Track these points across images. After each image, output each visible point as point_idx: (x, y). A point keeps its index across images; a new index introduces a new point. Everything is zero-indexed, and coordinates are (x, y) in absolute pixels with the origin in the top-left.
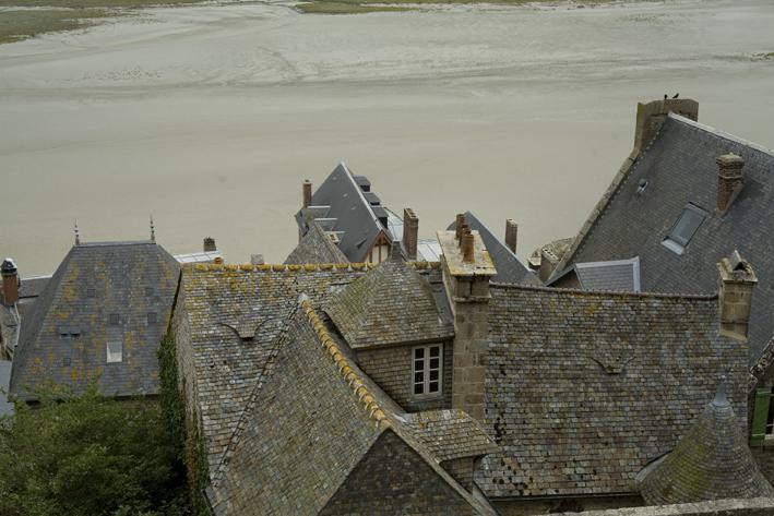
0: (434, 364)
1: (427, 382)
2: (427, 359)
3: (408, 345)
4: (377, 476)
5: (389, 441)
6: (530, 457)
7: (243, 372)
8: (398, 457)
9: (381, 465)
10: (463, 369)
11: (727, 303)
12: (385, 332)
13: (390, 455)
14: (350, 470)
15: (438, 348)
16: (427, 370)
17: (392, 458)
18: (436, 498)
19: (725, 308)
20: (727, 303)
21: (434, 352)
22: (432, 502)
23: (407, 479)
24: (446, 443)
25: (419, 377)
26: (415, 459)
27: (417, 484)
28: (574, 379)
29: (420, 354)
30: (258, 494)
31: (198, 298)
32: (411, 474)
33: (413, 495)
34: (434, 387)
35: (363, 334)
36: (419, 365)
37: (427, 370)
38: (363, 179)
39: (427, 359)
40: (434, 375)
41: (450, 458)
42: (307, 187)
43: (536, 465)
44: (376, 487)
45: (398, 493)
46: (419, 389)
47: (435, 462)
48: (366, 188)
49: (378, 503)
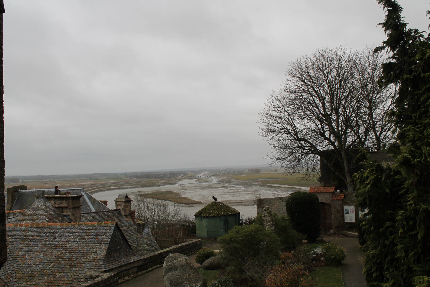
11: (126, 209)
19: (125, 211)
20: (126, 209)
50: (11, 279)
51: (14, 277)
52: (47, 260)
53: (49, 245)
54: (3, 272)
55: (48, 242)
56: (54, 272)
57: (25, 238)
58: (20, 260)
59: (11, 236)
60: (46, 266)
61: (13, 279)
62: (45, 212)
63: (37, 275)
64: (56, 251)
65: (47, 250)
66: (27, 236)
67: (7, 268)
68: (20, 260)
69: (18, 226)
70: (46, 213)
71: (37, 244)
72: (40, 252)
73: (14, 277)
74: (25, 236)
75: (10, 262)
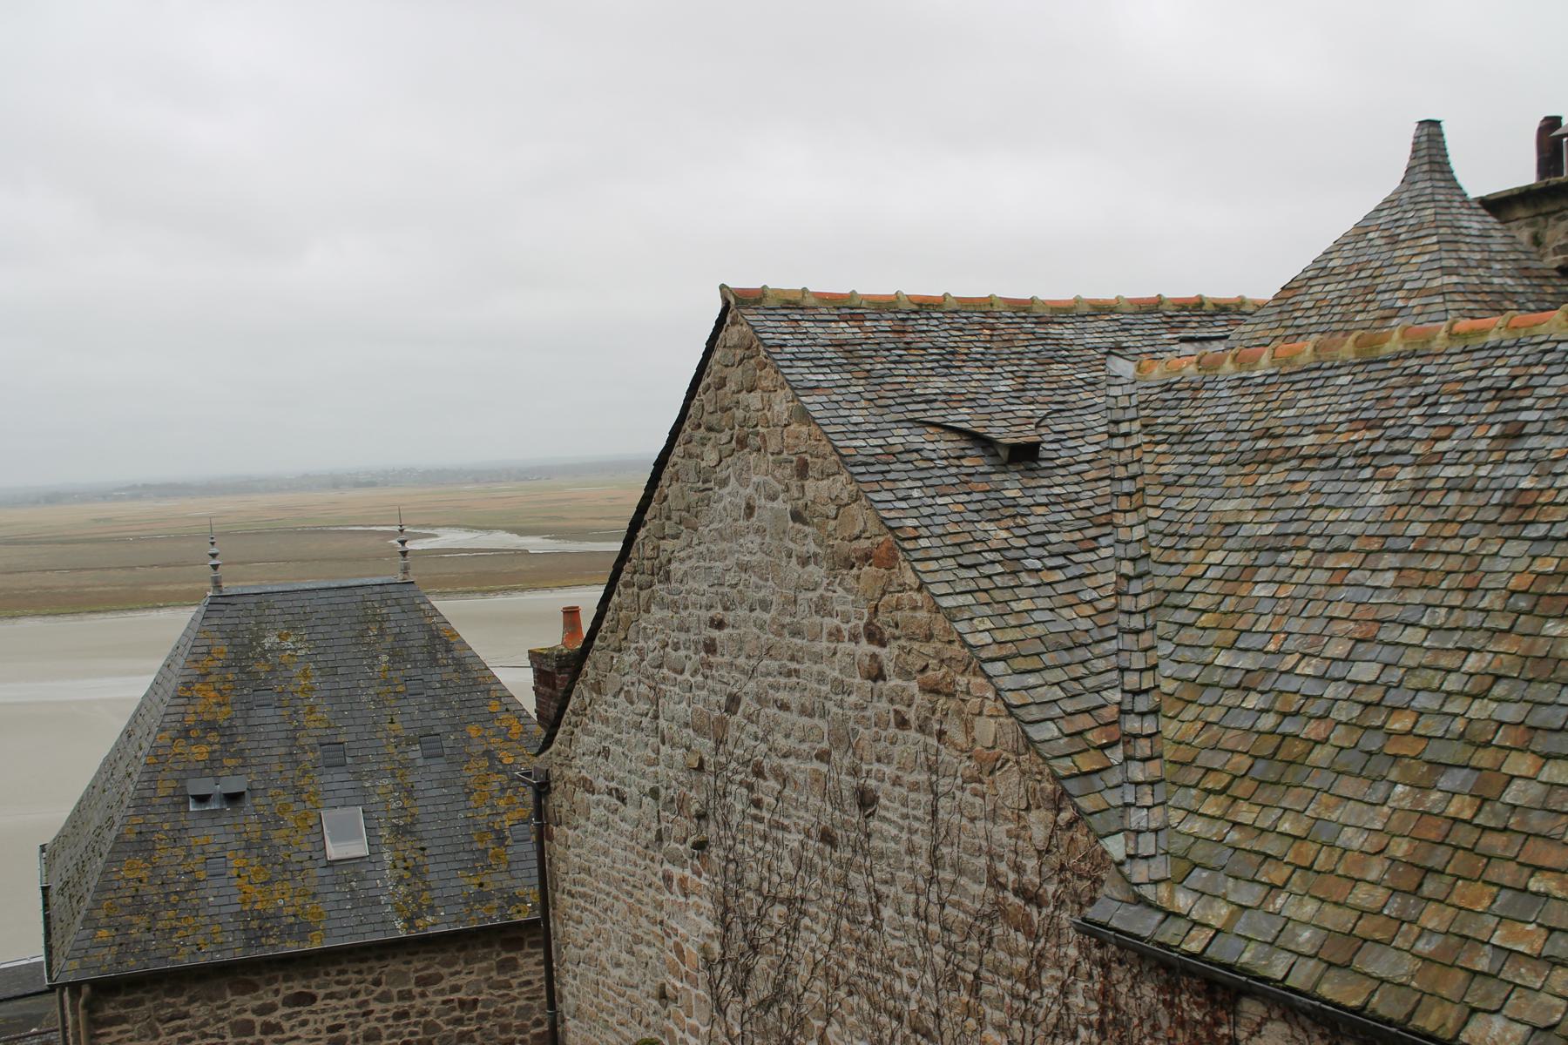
7: (1053, 538)
31: (817, 362)
50: (1116, 755)
51: (1143, 748)
52: (1430, 629)
53: (1453, 498)
54: (1062, 695)
55: (1450, 472)
56: (1488, 744)
57: (1262, 444)
58: (1204, 611)
59: (1174, 439)
60: (1414, 682)
61: (1128, 758)
62: (1447, 271)
63: (1320, 755)
64: (1512, 548)
65: (1428, 537)
66: (1278, 431)
67: (1101, 665)
68: (1204, 611)
69: (1228, 367)
70: (1455, 279)
71: (1348, 487)
72: (1368, 553)
73: (1143, 748)
74: (1268, 434)
75: (1137, 622)
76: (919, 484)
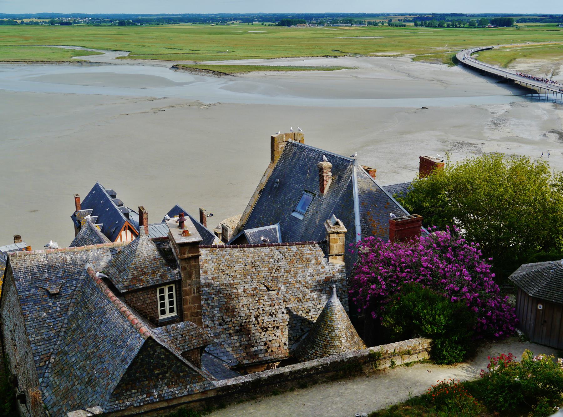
0: (171, 296)
1: (167, 307)
2: (166, 294)
3: (154, 287)
4: (145, 366)
5: (150, 345)
6: (232, 344)
8: (156, 353)
9: (147, 359)
10: (188, 297)
12: (140, 280)
13: (152, 353)
14: (128, 365)
15: (172, 287)
16: (167, 301)
17: (154, 354)
18: (181, 374)
21: (170, 289)
22: (179, 377)
23: (164, 365)
24: (183, 342)
25: (163, 305)
26: (167, 353)
27: (169, 368)
28: (252, 295)
29: (162, 291)
30: (72, 387)
32: (165, 362)
33: (168, 375)
34: (171, 310)
35: (126, 283)
36: (162, 298)
37: (167, 301)
38: (112, 191)
39: (166, 294)
40: (171, 303)
41: (186, 350)
42: (77, 200)
43: (235, 348)
44: (145, 373)
45: (158, 374)
46: (163, 312)
47: (178, 354)
48: (114, 196)
49: (147, 382)
76: (32, 303)
